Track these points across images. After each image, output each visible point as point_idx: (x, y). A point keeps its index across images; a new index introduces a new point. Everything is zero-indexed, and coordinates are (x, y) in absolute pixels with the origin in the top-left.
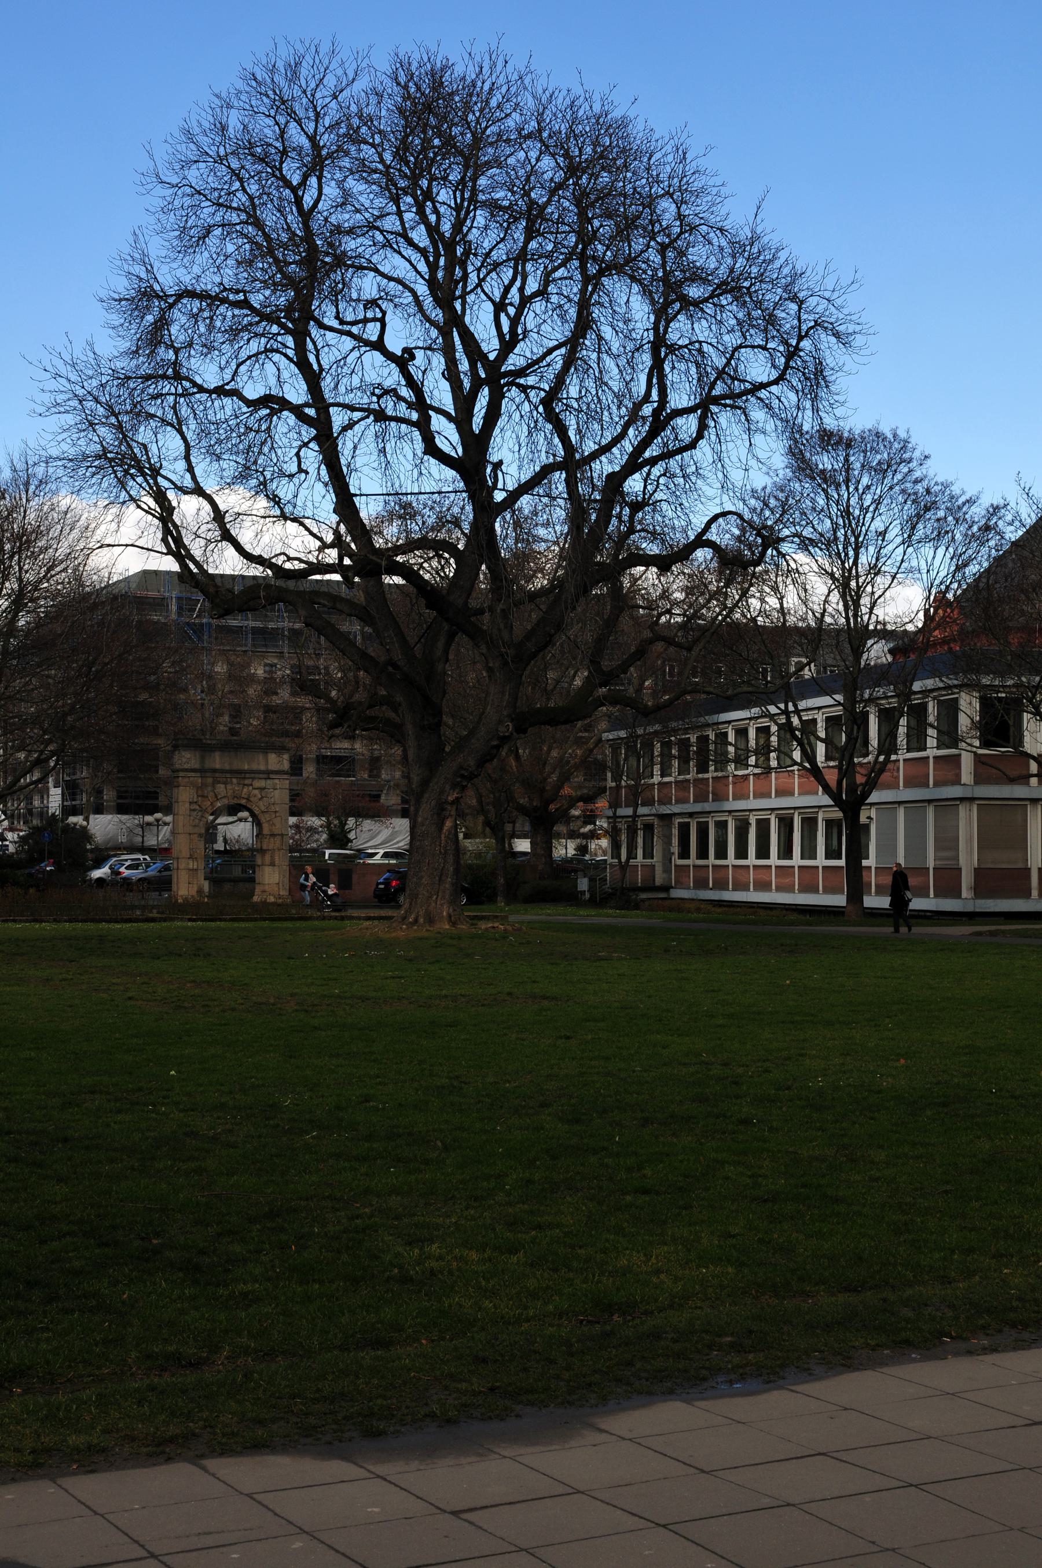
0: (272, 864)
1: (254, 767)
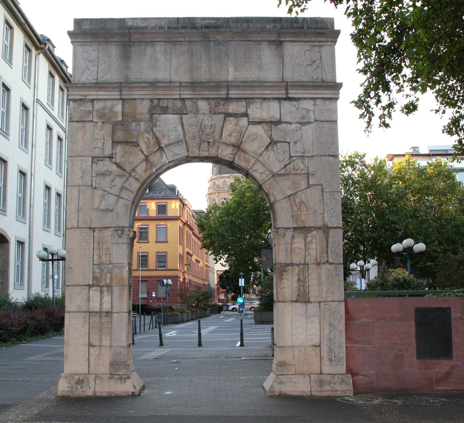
0: (303, 298)
1: (252, 74)
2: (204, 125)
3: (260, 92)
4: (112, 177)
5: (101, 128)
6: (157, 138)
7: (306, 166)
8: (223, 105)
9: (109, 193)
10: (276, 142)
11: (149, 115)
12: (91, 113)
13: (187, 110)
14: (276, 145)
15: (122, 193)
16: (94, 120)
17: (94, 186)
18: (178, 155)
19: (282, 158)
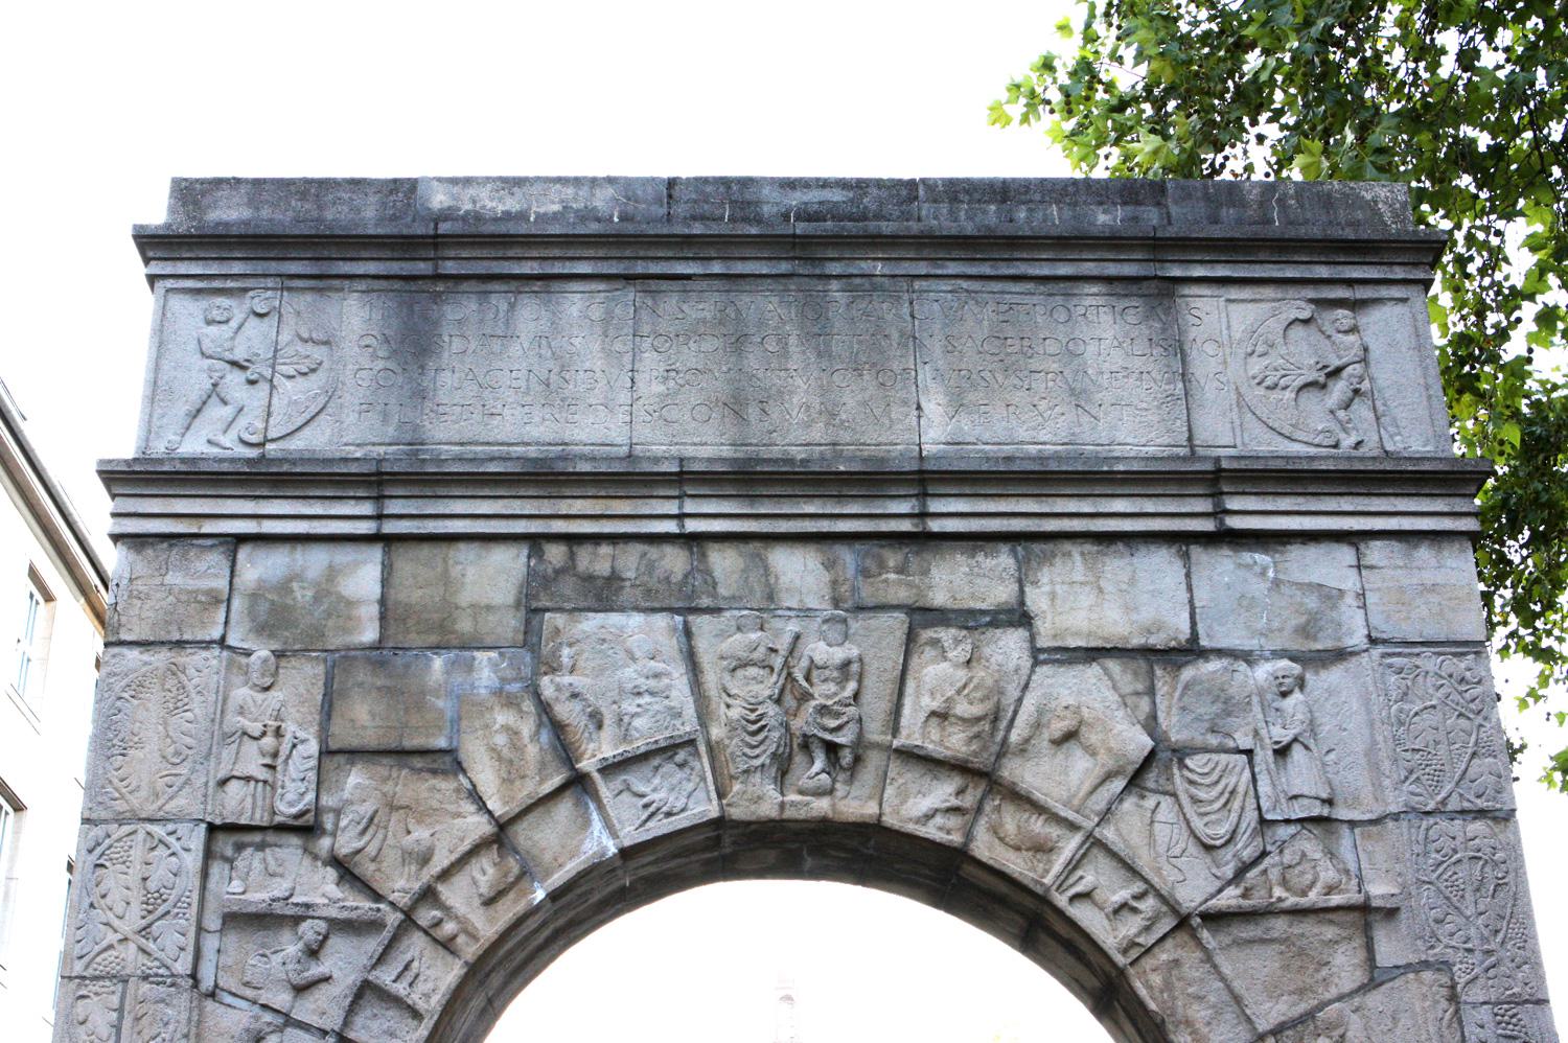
1: (1033, 426)
2: (805, 663)
3: (1086, 506)
4: (310, 930)
5: (268, 681)
6: (558, 728)
7: (1347, 872)
8: (900, 570)
9: (289, 1021)
10: (1181, 753)
11: (522, 613)
12: (218, 601)
13: (714, 596)
14: (1182, 765)
15: (359, 1020)
16: (231, 641)
17: (207, 983)
18: (669, 814)
19: (1223, 830)
